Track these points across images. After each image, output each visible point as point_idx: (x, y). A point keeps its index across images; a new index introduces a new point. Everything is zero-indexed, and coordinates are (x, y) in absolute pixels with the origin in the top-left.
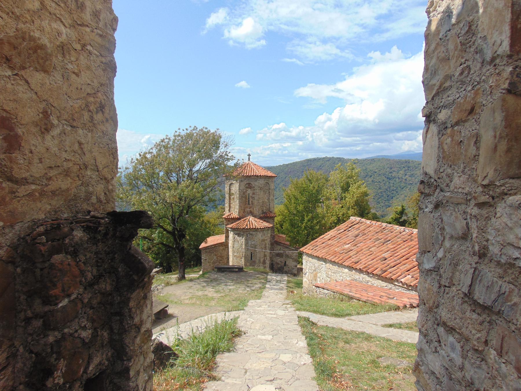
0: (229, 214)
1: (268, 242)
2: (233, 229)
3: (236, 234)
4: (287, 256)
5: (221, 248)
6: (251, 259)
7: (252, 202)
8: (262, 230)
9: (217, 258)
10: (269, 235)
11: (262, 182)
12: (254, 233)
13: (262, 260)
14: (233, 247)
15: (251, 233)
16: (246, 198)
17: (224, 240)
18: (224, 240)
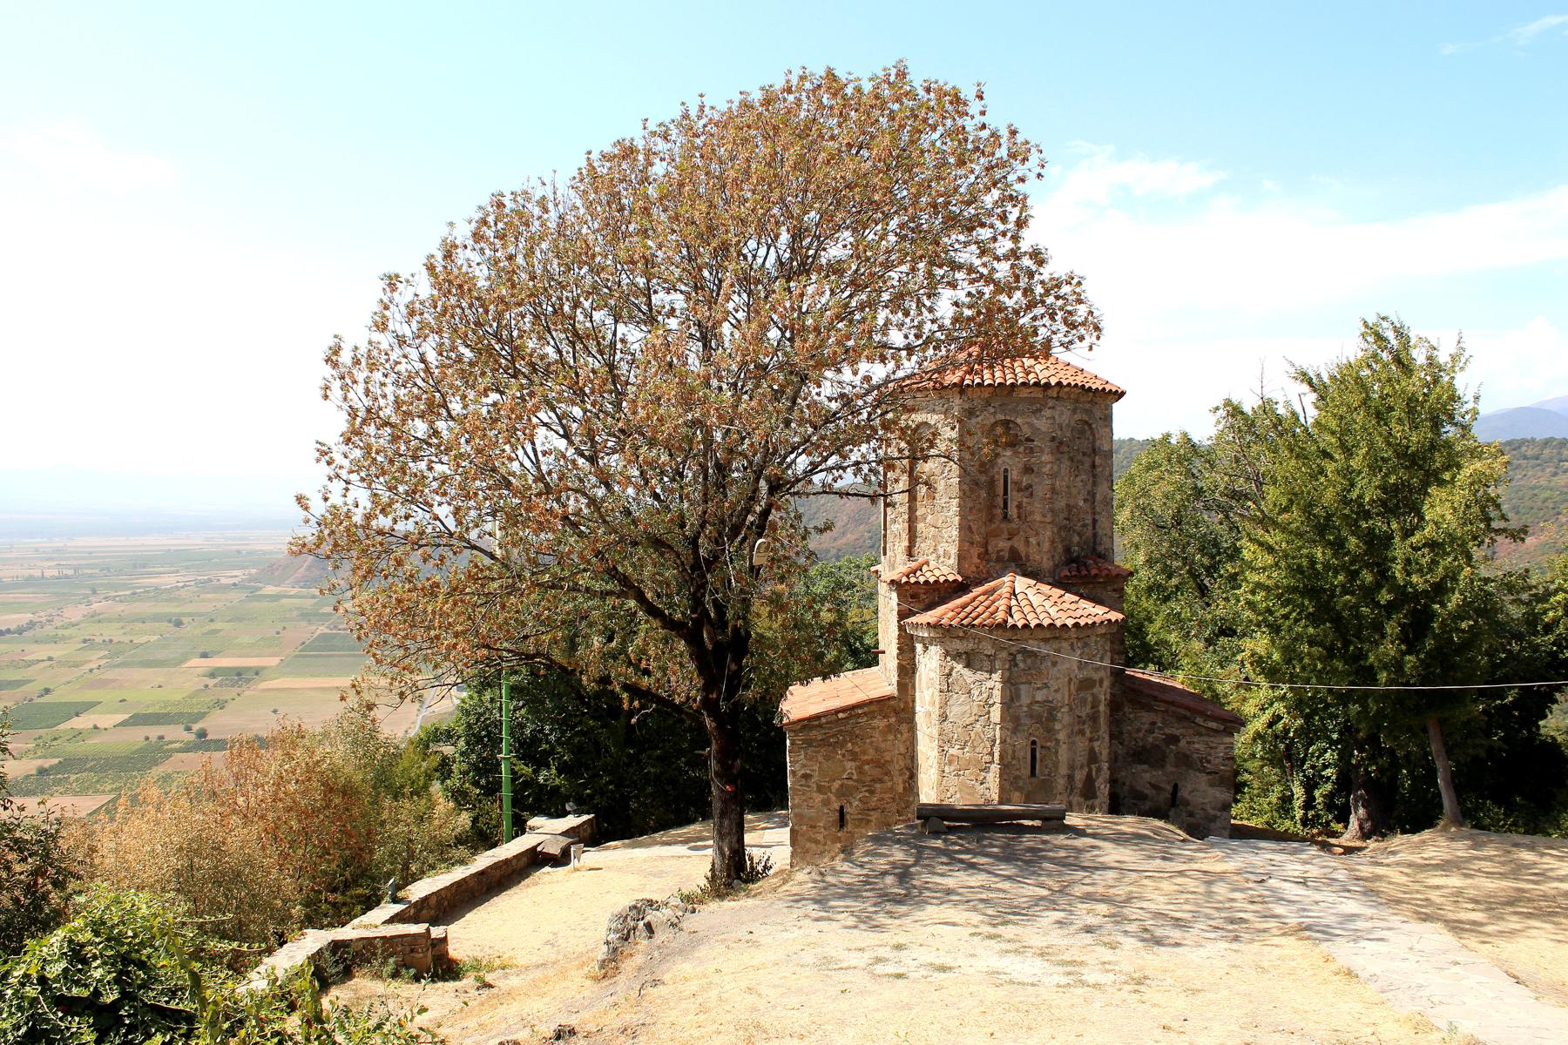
1: (1103, 692)
2: (943, 633)
3: (957, 656)
4: (1185, 760)
5: (879, 723)
6: (1033, 773)
7: (1019, 506)
8: (1082, 631)
9: (860, 770)
13: (1080, 776)
14: (944, 718)
15: (1032, 646)
16: (992, 483)
17: (892, 690)
18: (892, 690)
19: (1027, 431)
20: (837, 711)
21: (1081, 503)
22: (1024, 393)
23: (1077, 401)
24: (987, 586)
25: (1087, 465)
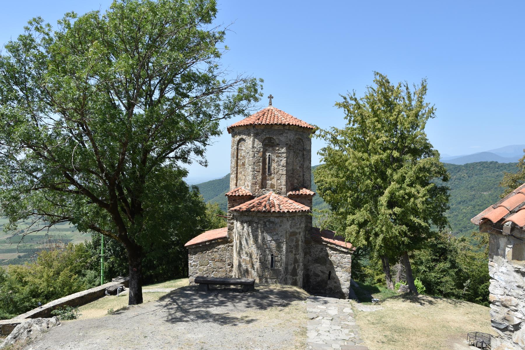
0: (236, 189)
1: (301, 237)
8: (292, 215)
10: (303, 225)
11: (291, 136)
12: (277, 220)
13: (290, 268)
15: (272, 219)
20: (206, 242)
21: (298, 168)
22: (276, 127)
23: (297, 131)
25: (301, 155)
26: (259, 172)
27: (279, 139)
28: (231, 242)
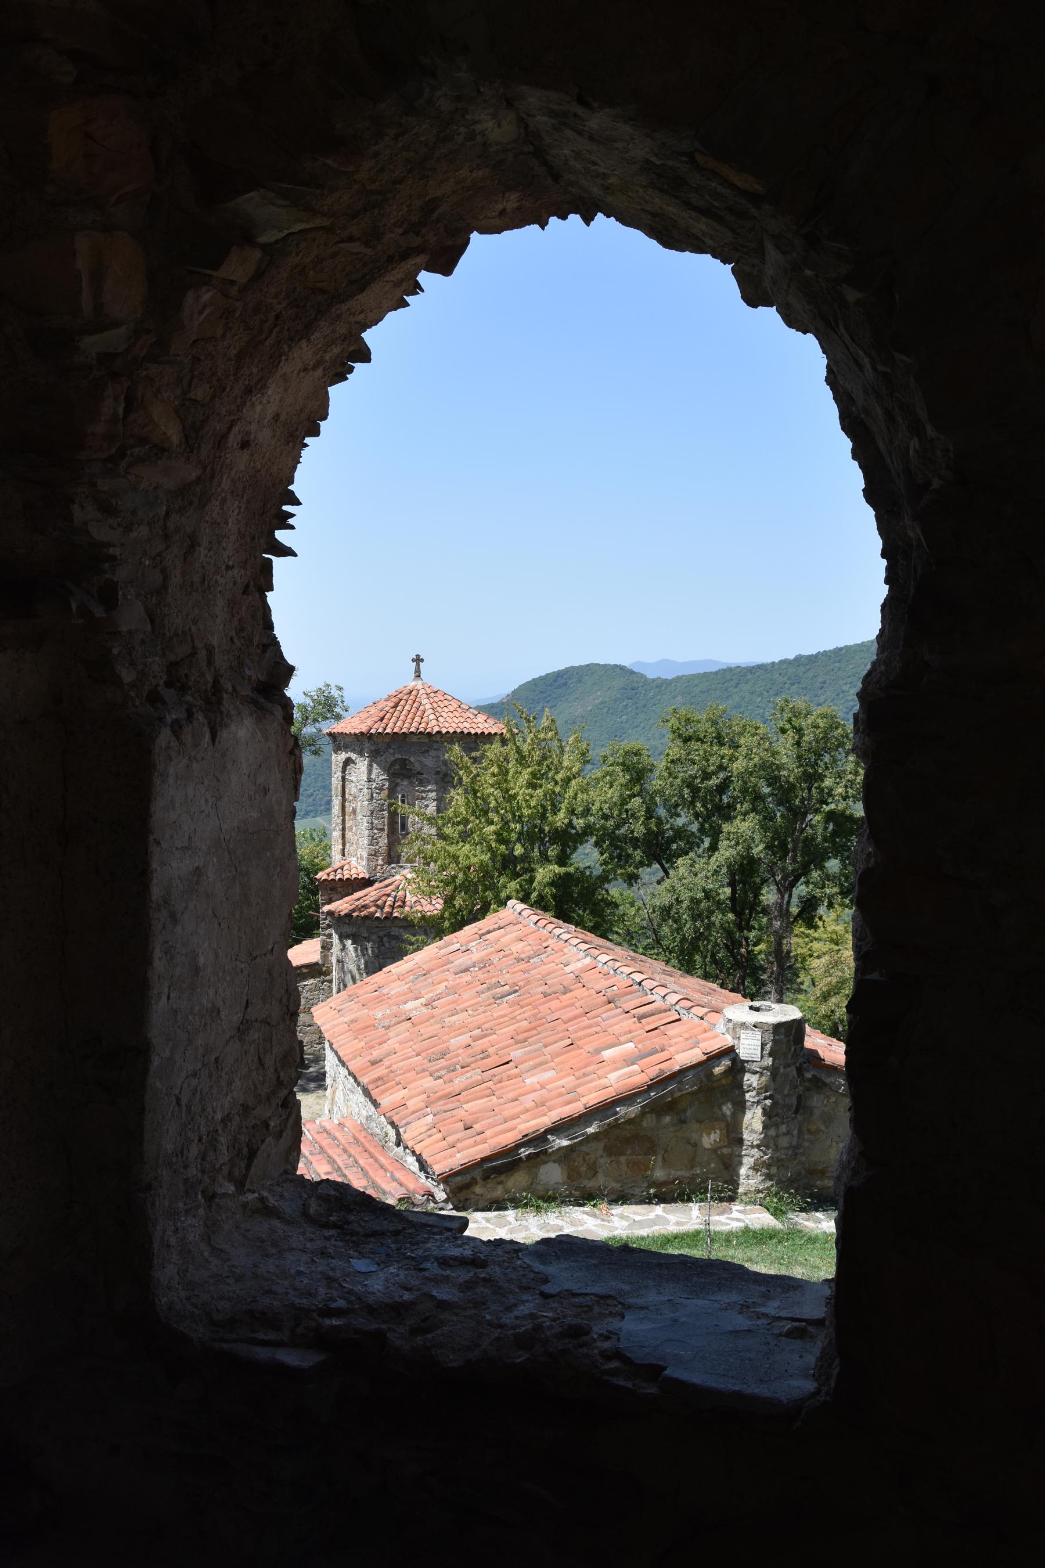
15: (395, 931)
19: (418, 767)
22: (415, 739)
24: (387, 882)
26: (382, 830)
27: (421, 762)
28: (329, 972)
